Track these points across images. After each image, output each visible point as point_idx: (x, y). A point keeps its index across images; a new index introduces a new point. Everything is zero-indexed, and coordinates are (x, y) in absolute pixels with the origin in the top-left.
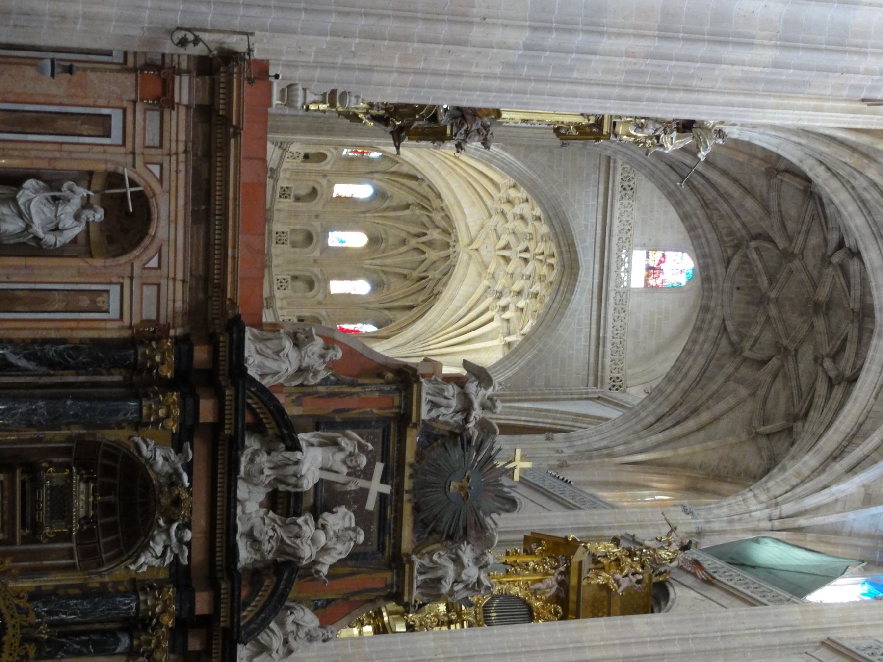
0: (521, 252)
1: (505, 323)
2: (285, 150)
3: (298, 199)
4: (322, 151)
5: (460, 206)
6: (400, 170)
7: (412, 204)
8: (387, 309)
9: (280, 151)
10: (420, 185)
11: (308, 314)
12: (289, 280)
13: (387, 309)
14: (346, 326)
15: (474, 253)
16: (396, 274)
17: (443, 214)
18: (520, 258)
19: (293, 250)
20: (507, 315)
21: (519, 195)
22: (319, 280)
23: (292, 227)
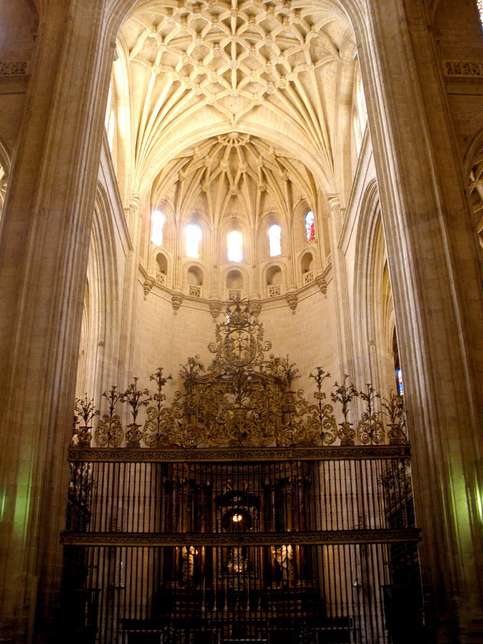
0: (231, 59)
1: (295, 69)
2: (153, 282)
3: (201, 284)
4: (155, 256)
5: (195, 133)
6: (173, 200)
7: (201, 189)
8: (291, 205)
9: (154, 288)
10: (184, 179)
11: (300, 266)
12: (271, 286)
13: (291, 205)
14: (309, 236)
15: (237, 117)
16: (262, 204)
17: (207, 157)
18: (237, 59)
19: (245, 287)
20: (288, 67)
21: (180, 58)
22: (269, 264)
23: (225, 287)
